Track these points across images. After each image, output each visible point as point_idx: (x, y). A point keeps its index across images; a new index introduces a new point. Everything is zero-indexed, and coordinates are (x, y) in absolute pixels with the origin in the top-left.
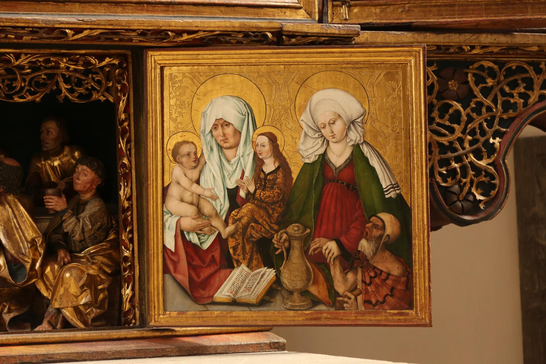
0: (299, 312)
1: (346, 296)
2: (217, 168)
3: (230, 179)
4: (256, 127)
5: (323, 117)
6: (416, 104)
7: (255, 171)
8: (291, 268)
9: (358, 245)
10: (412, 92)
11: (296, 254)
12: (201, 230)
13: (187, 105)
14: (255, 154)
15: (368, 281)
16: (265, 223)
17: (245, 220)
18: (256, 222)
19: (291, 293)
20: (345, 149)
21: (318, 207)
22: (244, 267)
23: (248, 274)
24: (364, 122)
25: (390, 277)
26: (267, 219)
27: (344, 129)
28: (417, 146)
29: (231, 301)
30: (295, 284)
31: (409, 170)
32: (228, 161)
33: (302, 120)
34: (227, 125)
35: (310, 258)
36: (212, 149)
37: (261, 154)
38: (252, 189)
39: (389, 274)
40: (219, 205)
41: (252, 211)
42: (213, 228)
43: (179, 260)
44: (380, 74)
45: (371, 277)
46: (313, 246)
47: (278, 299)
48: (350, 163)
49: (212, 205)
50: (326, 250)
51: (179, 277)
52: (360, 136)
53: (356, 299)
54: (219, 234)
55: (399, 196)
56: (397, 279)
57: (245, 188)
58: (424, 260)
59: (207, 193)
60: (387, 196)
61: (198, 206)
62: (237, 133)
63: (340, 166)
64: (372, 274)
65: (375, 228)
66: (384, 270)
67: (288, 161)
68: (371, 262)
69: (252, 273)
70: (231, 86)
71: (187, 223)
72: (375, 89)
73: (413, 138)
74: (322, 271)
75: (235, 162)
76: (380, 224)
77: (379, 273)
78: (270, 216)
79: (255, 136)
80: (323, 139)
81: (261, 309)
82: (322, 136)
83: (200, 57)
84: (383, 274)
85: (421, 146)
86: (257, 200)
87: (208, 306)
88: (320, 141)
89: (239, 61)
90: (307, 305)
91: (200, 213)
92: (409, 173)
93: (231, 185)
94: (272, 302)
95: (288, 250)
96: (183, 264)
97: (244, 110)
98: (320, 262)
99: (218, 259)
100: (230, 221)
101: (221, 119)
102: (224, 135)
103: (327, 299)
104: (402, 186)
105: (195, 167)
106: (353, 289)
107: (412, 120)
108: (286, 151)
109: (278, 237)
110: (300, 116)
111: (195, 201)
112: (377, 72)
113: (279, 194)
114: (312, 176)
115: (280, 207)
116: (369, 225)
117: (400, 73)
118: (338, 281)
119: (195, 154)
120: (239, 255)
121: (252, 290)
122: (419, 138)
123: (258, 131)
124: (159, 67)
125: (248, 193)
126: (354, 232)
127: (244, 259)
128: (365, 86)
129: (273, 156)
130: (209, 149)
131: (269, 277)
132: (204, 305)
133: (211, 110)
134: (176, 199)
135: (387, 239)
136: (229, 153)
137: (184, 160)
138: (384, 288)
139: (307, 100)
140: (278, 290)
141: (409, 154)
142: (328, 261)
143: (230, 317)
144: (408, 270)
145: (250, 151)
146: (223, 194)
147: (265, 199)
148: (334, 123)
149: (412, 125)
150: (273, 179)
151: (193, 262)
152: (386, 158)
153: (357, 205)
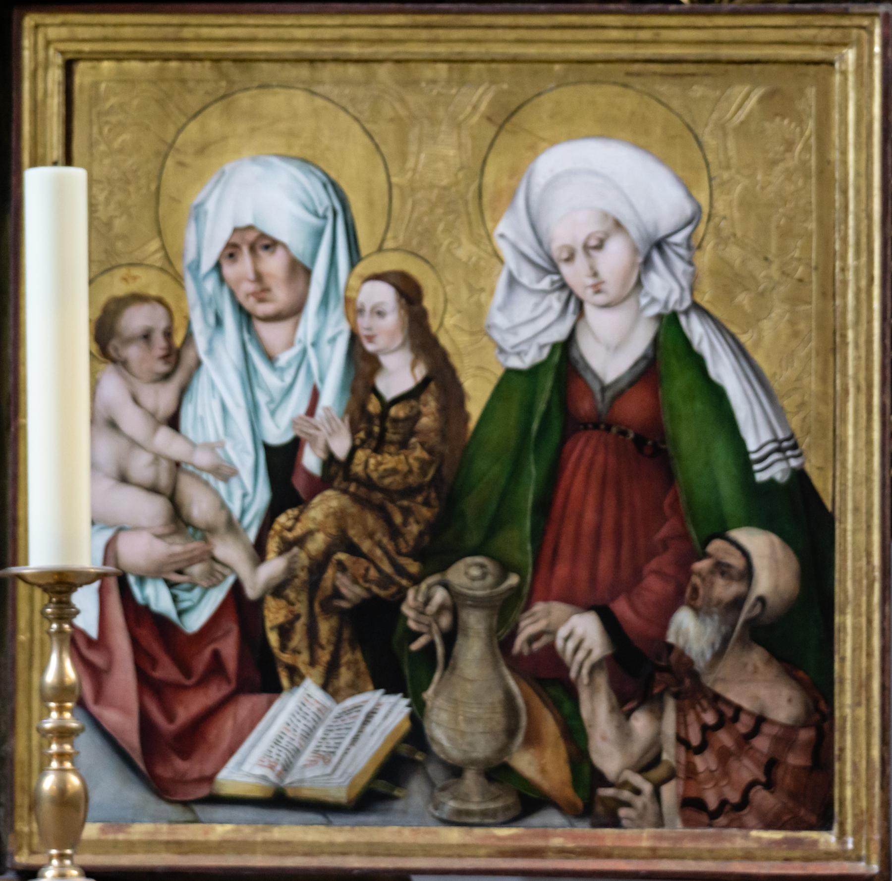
0: (479, 832)
1: (625, 785)
2: (234, 381)
3: (273, 413)
4: (358, 251)
5: (567, 227)
6: (858, 191)
7: (353, 391)
8: (458, 695)
9: (665, 627)
10: (844, 153)
11: (473, 650)
12: (180, 572)
13: (143, 181)
14: (354, 339)
15: (695, 738)
16: (378, 552)
17: (317, 544)
18: (353, 550)
19: (456, 771)
20: (632, 328)
21: (544, 507)
22: (310, 690)
23: (322, 712)
24: (695, 243)
25: (766, 729)
26: (385, 540)
27: (633, 265)
28: (857, 322)
29: (268, 794)
30: (470, 744)
31: (834, 399)
32: (270, 359)
33: (502, 236)
34: (267, 247)
35: (517, 664)
36: (219, 322)
37: (371, 339)
38: (341, 447)
39: (760, 720)
40: (237, 494)
41: (340, 516)
42: (218, 567)
43: (110, 663)
44: (747, 96)
45: (705, 729)
46: (528, 627)
47: (416, 792)
48: (648, 371)
49: (216, 493)
50: (567, 639)
51: (110, 717)
52: (682, 289)
53: (657, 794)
54: (237, 588)
55: (800, 477)
56: (786, 736)
57: (321, 444)
58: (869, 676)
59: (202, 459)
60: (761, 477)
61: (173, 499)
62: (299, 271)
63: (617, 381)
64: (710, 718)
65: (723, 574)
66: (746, 704)
67: (455, 361)
68: (708, 681)
69: (337, 709)
70: (282, 126)
71: (138, 550)
72: (731, 144)
73: (844, 296)
74: (555, 706)
75: (289, 364)
76: (736, 561)
77: (728, 715)
78: (395, 533)
79: (354, 282)
80: (564, 295)
81: (361, 818)
82: (563, 286)
83: (187, 33)
84: (744, 718)
85: (870, 322)
86: (357, 479)
87: (198, 809)
88: (555, 302)
89: (310, 49)
90: (506, 809)
91: (178, 519)
92: (831, 407)
93: (277, 433)
94: (396, 798)
95: (450, 637)
96: (124, 677)
97: (323, 200)
98: (547, 675)
99: (231, 665)
100: (273, 545)
101: (250, 228)
102: (259, 277)
103: (569, 792)
104: (809, 447)
105: (166, 377)
106: (649, 764)
107: (844, 240)
108: (449, 331)
109: (421, 599)
110: (496, 221)
111: (164, 481)
112: (739, 91)
113: (424, 465)
114: (529, 409)
115: (426, 503)
116: (702, 565)
117: (811, 92)
118: (604, 738)
119: (168, 334)
120: (296, 652)
121: (335, 760)
122: (863, 296)
123: (362, 268)
124: (59, 60)
125: (330, 460)
126: (655, 586)
127: (313, 662)
128: (698, 131)
129: (408, 345)
130: (212, 320)
131: (390, 719)
132: (186, 804)
133: (220, 201)
134: (107, 476)
135: (757, 610)
136: (271, 333)
137: (133, 353)
138: (746, 762)
139: (518, 172)
140: (415, 762)
141: (832, 347)
142: (573, 674)
143: (265, 843)
144: (823, 706)
145: (338, 327)
146: (250, 461)
147: (382, 477)
148: (600, 246)
149: (844, 258)
150: (407, 419)
151: (154, 669)
152: (759, 358)
153: (667, 501)
